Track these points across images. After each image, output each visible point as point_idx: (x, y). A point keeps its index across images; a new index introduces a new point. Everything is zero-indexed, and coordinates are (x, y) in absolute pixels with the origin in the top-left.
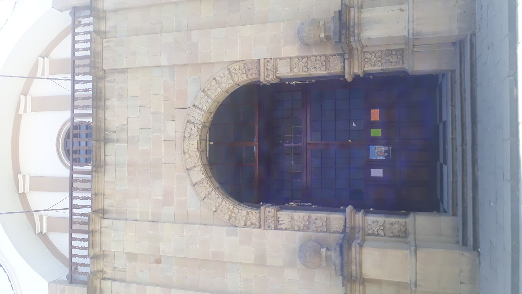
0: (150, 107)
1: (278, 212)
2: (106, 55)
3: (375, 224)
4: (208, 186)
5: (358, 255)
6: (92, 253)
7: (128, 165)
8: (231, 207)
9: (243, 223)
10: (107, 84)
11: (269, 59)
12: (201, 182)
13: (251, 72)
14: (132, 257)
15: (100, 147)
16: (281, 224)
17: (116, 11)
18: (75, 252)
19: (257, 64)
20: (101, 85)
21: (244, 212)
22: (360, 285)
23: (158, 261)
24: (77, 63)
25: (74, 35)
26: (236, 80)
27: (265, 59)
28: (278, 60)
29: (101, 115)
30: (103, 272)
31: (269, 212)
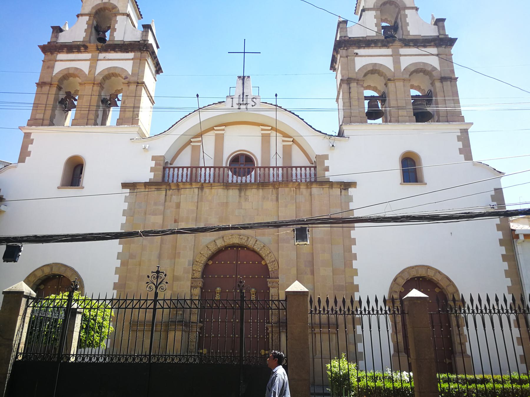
0: (257, 215)
1: (199, 288)
2: (287, 190)
3: (194, 337)
4: (214, 249)
5: (179, 329)
6: (179, 184)
7: (227, 203)
8: (202, 262)
9: (194, 269)
10: (271, 190)
12: (216, 245)
13: (273, 273)
14: (178, 206)
15: (237, 186)
16: (193, 289)
18: (181, 169)
20: (270, 187)
21: (200, 270)
22: (164, 329)
23: (176, 221)
24: (285, 169)
25: (301, 167)
26: (269, 265)
28: (278, 289)
29: (254, 187)
31: (200, 283)
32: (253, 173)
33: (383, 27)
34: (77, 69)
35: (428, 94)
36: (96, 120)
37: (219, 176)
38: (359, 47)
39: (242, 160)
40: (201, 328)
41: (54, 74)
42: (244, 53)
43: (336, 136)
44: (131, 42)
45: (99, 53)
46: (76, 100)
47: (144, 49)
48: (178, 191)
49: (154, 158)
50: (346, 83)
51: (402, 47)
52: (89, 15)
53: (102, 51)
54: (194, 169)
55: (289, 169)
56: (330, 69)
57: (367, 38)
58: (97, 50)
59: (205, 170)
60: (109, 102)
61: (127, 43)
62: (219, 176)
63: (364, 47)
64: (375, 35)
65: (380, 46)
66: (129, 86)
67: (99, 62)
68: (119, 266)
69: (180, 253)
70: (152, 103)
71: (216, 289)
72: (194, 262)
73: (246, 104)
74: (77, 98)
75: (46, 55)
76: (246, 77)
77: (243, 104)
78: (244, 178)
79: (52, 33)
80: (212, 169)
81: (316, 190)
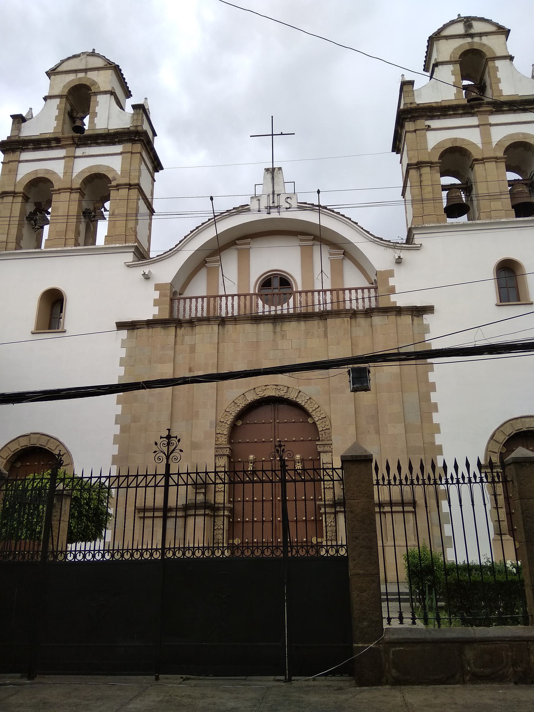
0: (299, 357)
1: (226, 457)
2: (338, 321)
8: (229, 423)
10: (316, 322)
11: (331, 448)
12: (246, 400)
14: (193, 349)
15: (270, 319)
17: (372, 326)
19: (329, 439)
21: (226, 433)
23: (190, 370)
25: (356, 289)
26: (317, 423)
27: (332, 444)
30: (181, 327)
32: (291, 301)
33: (465, 88)
34: (47, 171)
35: (532, 177)
36: (76, 240)
37: (245, 306)
38: (432, 117)
39: (276, 283)
40: (232, 510)
41: (18, 180)
42: (272, 135)
43: (404, 244)
44: (117, 130)
45: (76, 148)
46: (49, 213)
47: (137, 138)
48: (192, 329)
49: (158, 287)
50: (414, 168)
51: (492, 113)
52: (60, 96)
53: (80, 144)
54: (212, 299)
55: (341, 292)
56: (392, 151)
57: (443, 104)
58: (73, 144)
59: (227, 300)
60: (93, 214)
61: (112, 131)
62: (245, 306)
63: (438, 117)
64: (454, 99)
65: (461, 114)
66: (118, 189)
67: (77, 160)
68: (118, 433)
69: (198, 412)
70: (151, 213)
71: (248, 457)
72: (218, 423)
73: (277, 206)
74: (50, 210)
75: (6, 154)
76: (277, 169)
77: (274, 207)
78: (279, 307)
79: (13, 124)
80: (236, 298)
81: (377, 320)
